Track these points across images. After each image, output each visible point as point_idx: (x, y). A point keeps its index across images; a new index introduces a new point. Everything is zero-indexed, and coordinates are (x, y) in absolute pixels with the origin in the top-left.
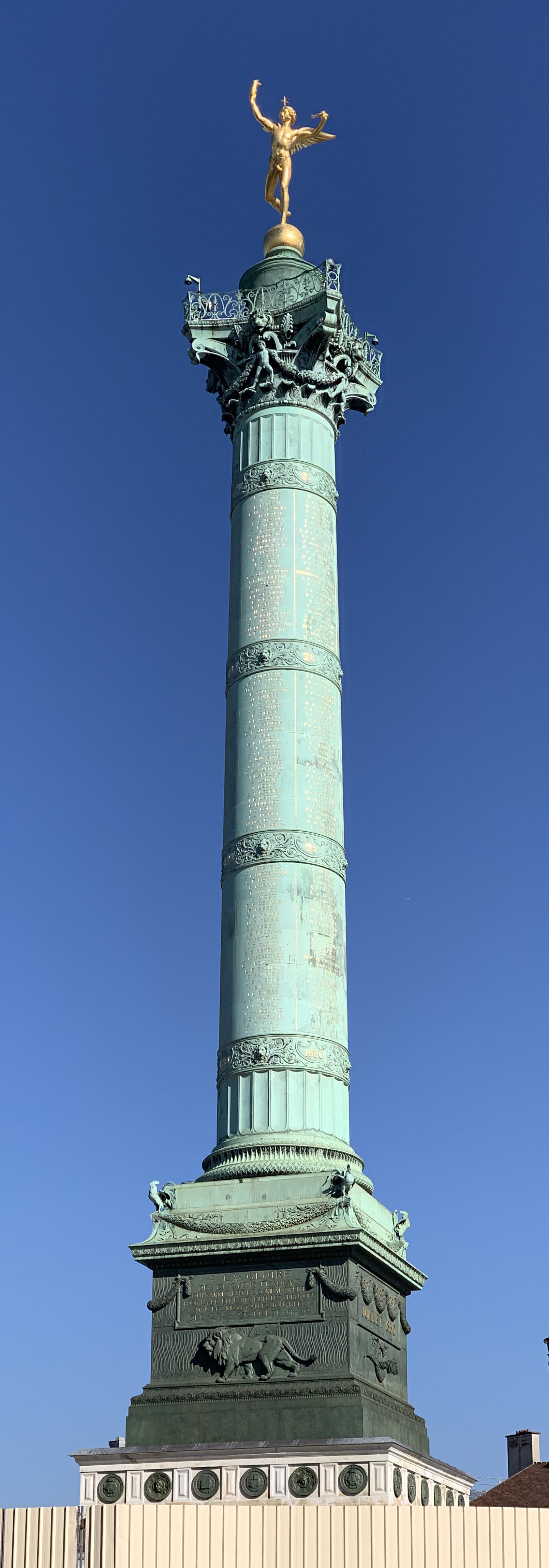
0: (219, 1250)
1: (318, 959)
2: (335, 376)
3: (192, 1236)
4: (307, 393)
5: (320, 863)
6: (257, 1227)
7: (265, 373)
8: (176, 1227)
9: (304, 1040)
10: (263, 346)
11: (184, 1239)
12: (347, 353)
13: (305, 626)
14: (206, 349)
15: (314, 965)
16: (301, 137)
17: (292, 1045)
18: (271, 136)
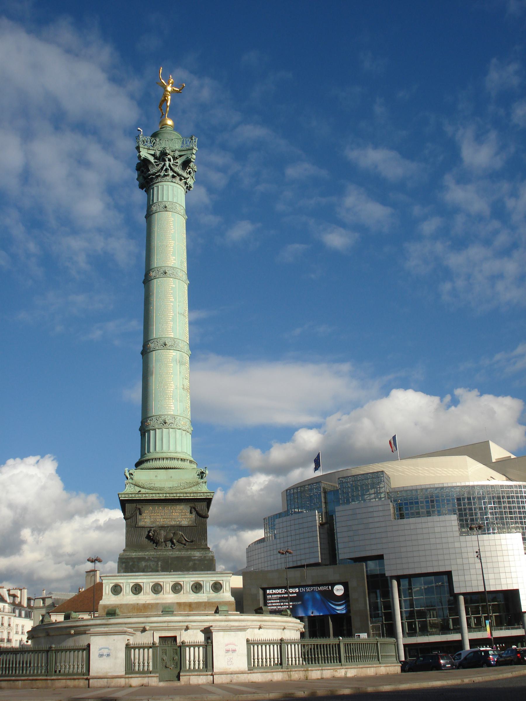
0: (156, 497)
4: (181, 180)
7: (166, 170)
8: (136, 487)
9: (182, 418)
10: (167, 160)
18: (165, 88)
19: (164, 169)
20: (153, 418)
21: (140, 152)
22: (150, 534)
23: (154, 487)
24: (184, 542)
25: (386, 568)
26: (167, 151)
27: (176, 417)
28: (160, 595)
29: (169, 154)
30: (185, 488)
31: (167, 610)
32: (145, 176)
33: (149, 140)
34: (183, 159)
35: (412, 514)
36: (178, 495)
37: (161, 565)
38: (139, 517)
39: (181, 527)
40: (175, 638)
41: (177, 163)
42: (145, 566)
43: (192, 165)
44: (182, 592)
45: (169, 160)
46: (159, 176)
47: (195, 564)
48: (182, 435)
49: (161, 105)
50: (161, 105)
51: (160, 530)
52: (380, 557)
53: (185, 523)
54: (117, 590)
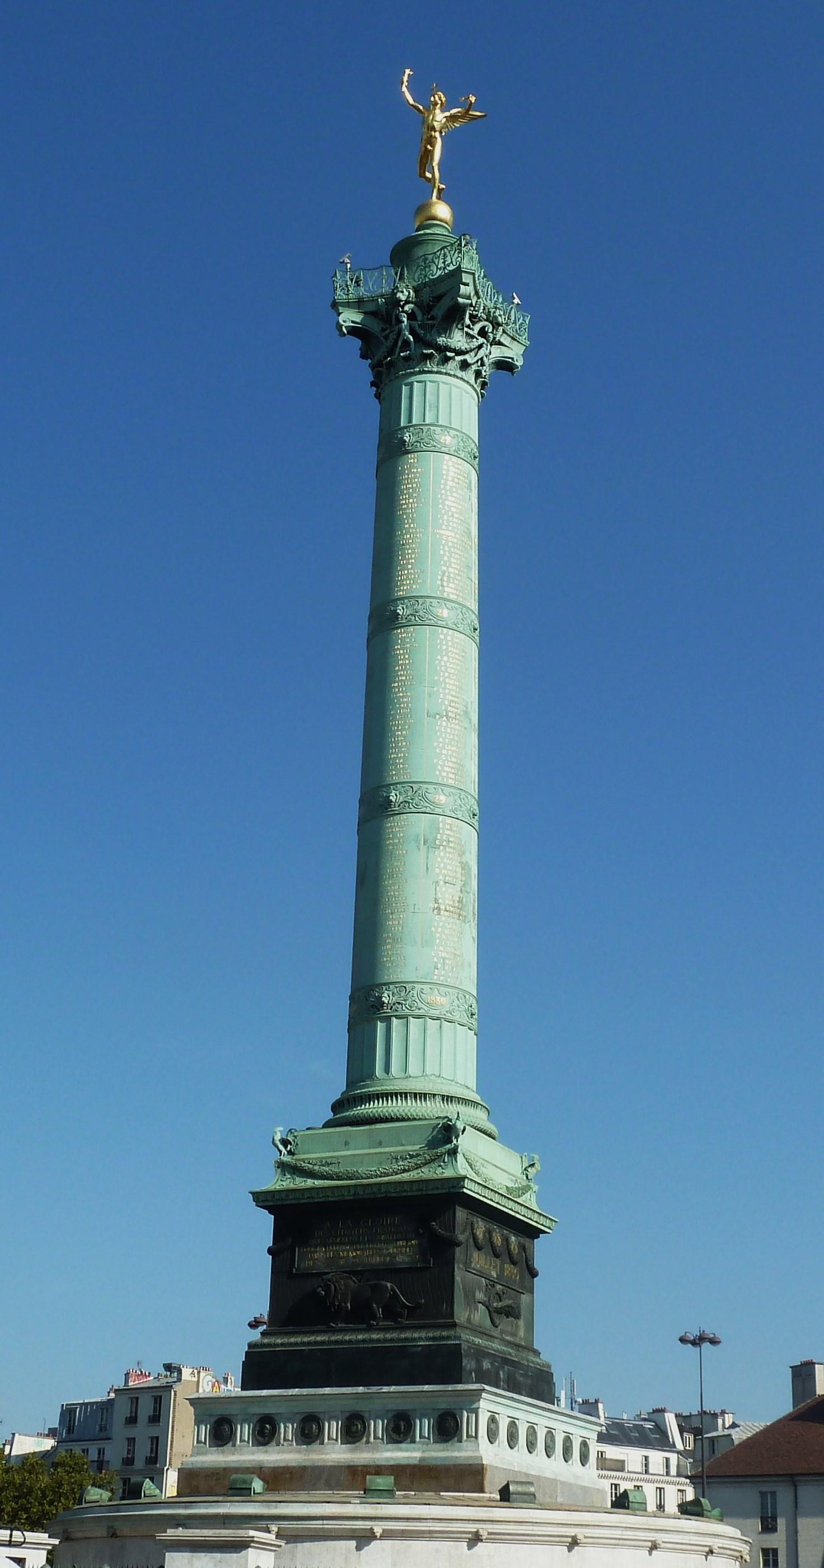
1: (442, 907)
2: (475, 343)
3: (310, 1183)
4: (446, 360)
5: (448, 813)
12: (487, 320)
13: (439, 583)
14: (353, 322)
15: (439, 914)
16: (452, 118)
26: (399, 295)
27: (409, 986)
29: (407, 302)
30: (404, 1171)
34: (445, 304)
36: (383, 1190)
39: (391, 1271)
41: (433, 318)
46: (391, 364)
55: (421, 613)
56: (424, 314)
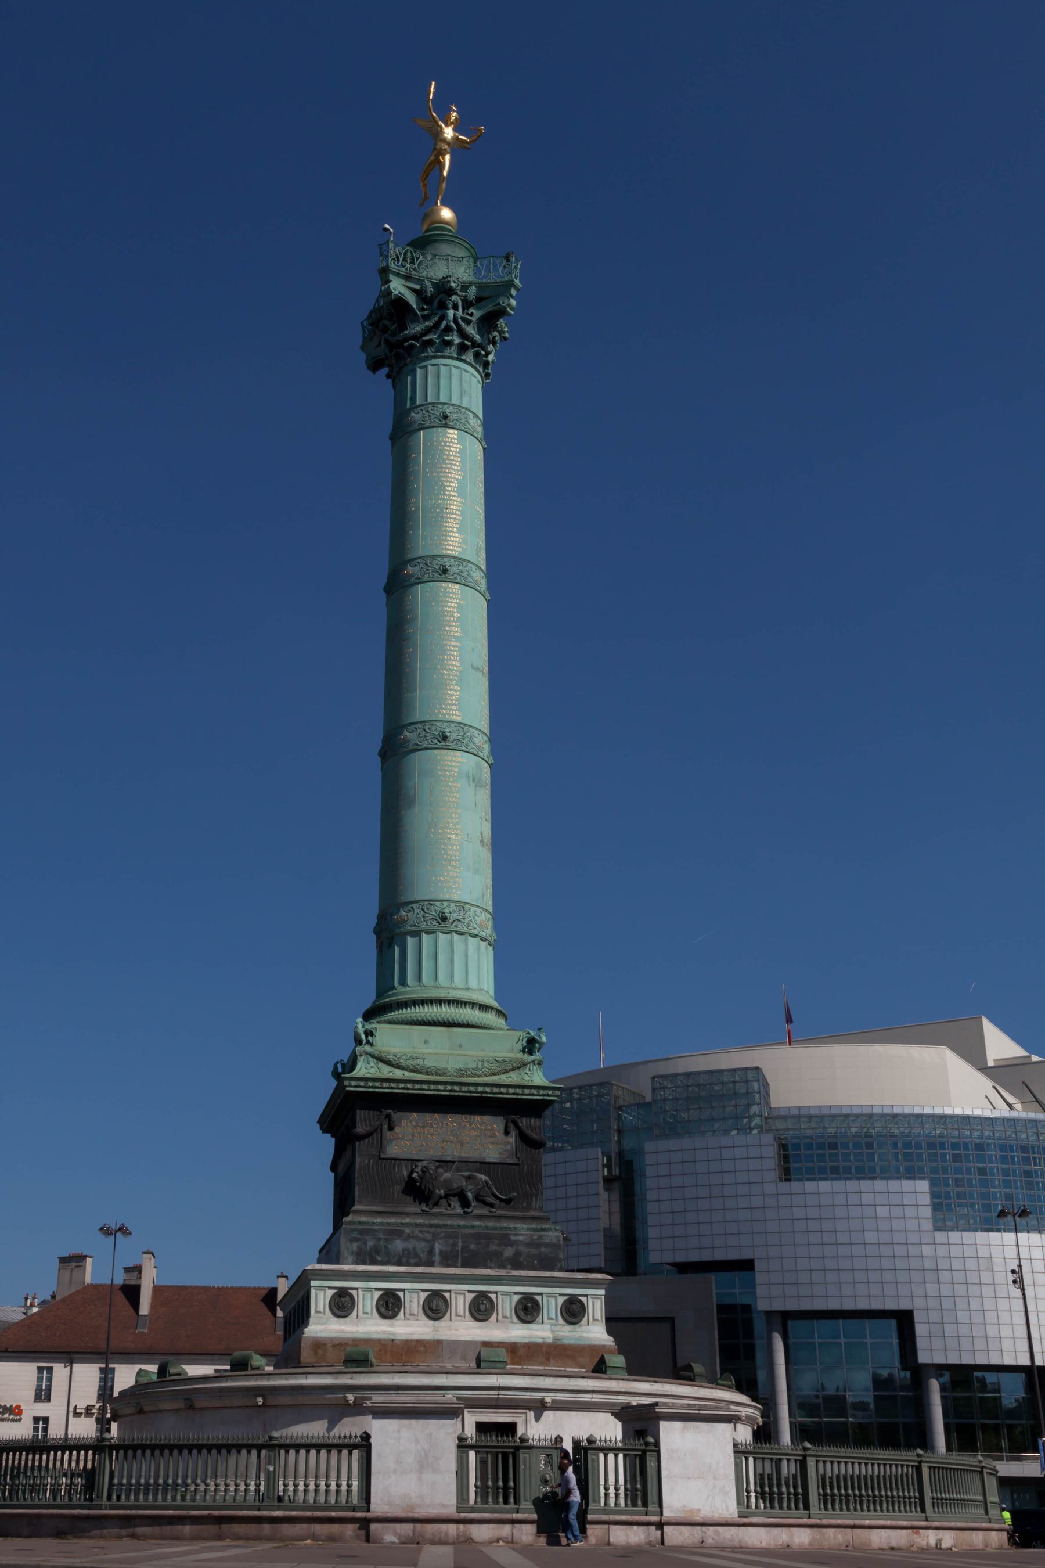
0: (429, 1091)
6: (461, 1072)
7: (448, 329)
8: (381, 1064)
11: (390, 1075)
17: (470, 913)
18: (438, 134)
19: (443, 326)
20: (415, 906)
21: (388, 282)
22: (415, 1175)
23: (423, 1068)
24: (491, 1200)
25: (760, 1291)
26: (453, 284)
27: (466, 906)
28: (442, 1324)
29: (456, 294)
30: (494, 1074)
31: (484, 1358)
32: (393, 340)
33: (409, 255)
34: (489, 307)
35: (847, 1170)
37: (441, 1251)
38: (388, 1134)
39: (484, 1166)
40: (511, 1428)
41: (471, 314)
42: (404, 1250)
43: (501, 322)
44: (493, 1318)
45: (455, 307)
46: (430, 343)
47: (517, 1254)
48: (479, 948)
49: (427, 174)
50: (427, 174)
51: (438, 1167)
52: (747, 1265)
53: (493, 1155)
54: (342, 1304)
55: (464, 574)
56: (463, 310)
